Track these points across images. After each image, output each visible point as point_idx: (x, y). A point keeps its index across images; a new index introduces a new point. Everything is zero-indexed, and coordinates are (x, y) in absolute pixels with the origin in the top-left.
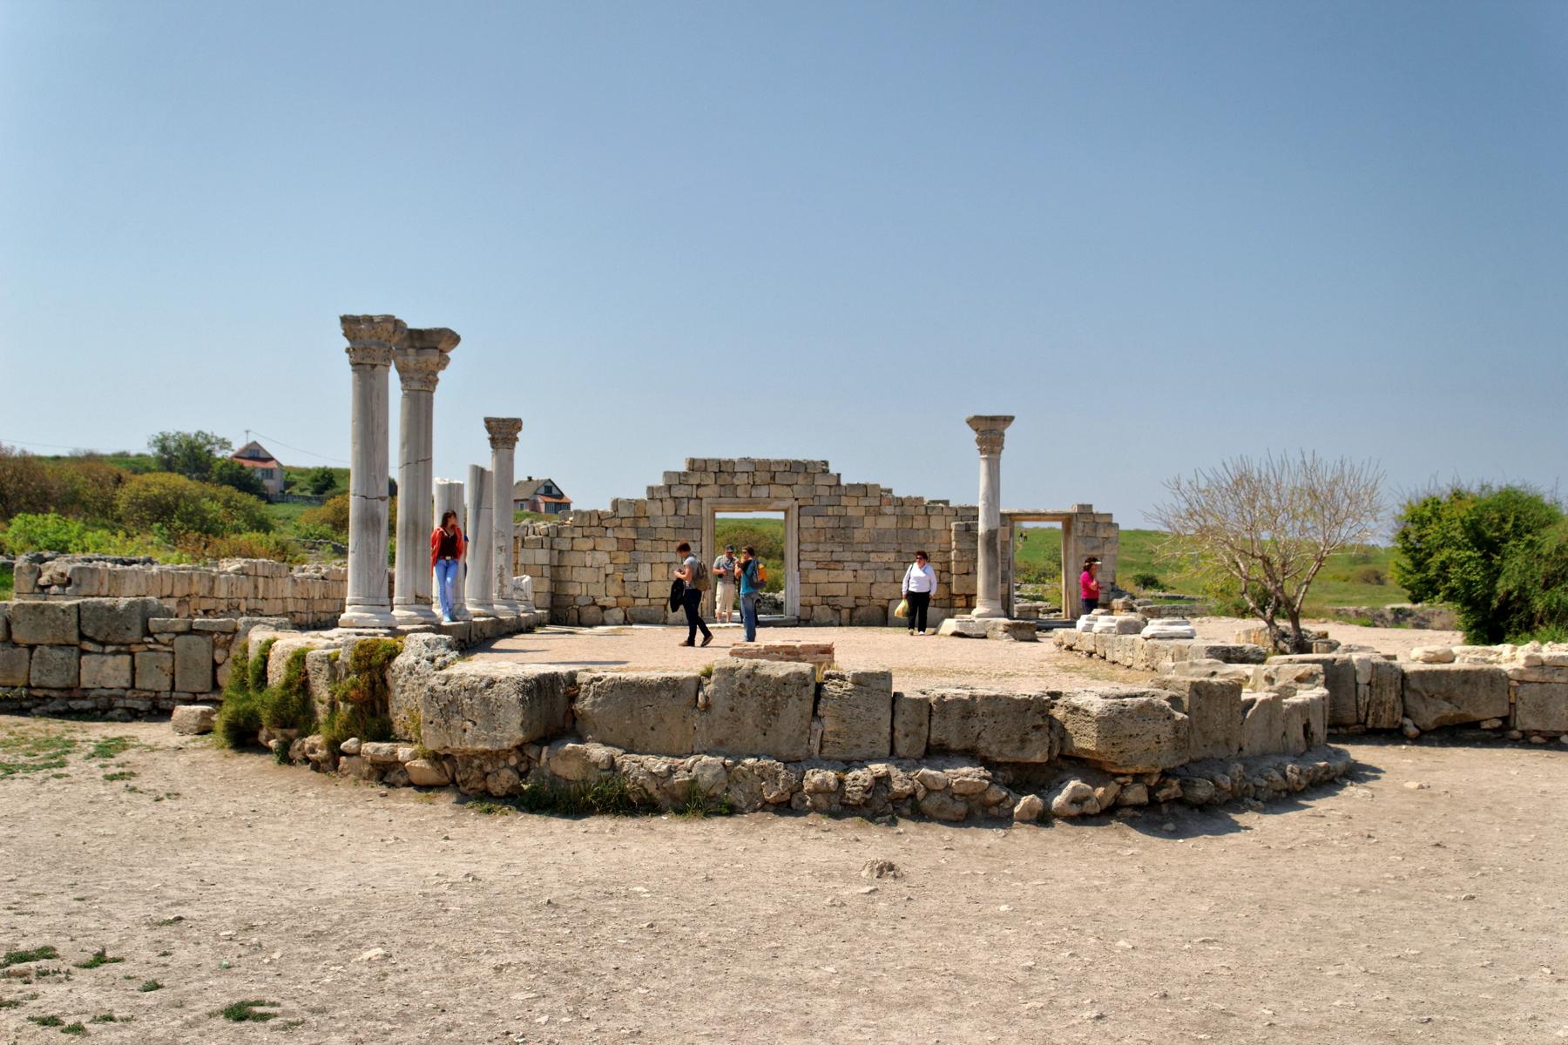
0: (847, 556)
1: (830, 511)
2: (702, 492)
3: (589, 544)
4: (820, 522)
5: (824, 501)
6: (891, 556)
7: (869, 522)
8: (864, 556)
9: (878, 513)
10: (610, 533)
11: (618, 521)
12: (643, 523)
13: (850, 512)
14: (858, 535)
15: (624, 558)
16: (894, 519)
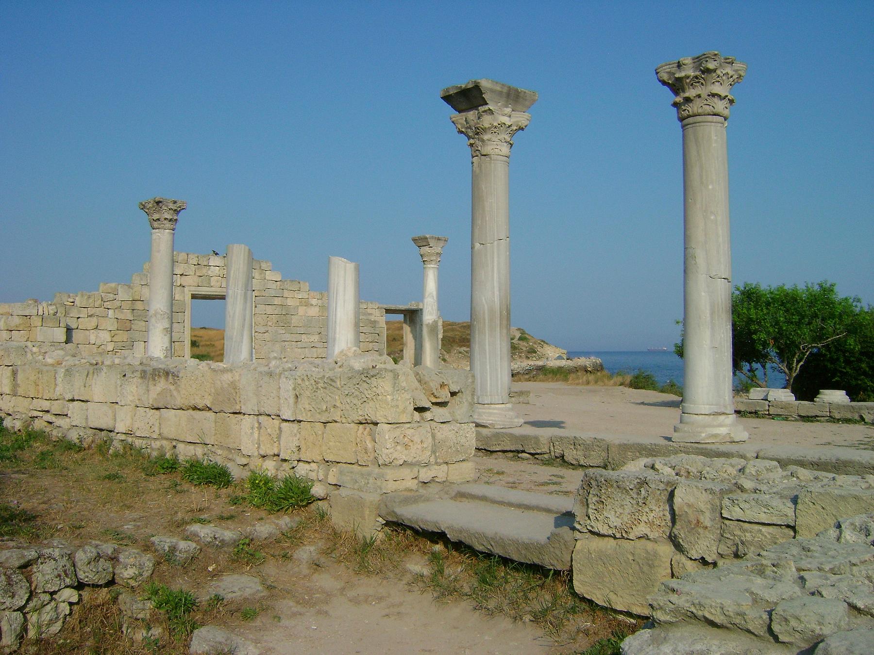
0: (288, 337)
1: (277, 301)
2: (185, 281)
3: (94, 322)
4: (269, 310)
5: (273, 293)
6: (316, 338)
7: (301, 310)
8: (297, 337)
9: (308, 305)
10: (111, 312)
11: (118, 304)
12: (139, 306)
13: (290, 302)
14: (295, 320)
15: (123, 336)
16: (317, 309)
